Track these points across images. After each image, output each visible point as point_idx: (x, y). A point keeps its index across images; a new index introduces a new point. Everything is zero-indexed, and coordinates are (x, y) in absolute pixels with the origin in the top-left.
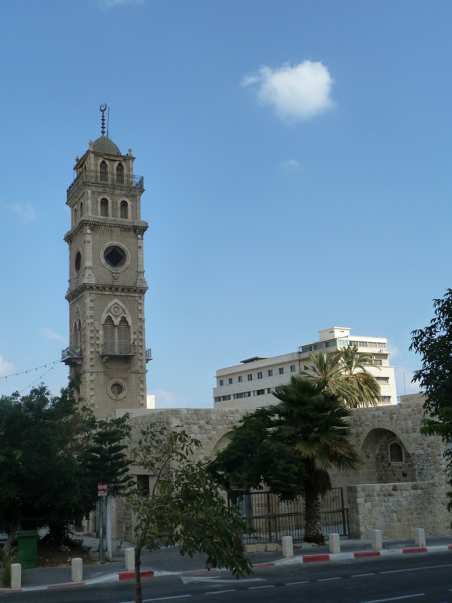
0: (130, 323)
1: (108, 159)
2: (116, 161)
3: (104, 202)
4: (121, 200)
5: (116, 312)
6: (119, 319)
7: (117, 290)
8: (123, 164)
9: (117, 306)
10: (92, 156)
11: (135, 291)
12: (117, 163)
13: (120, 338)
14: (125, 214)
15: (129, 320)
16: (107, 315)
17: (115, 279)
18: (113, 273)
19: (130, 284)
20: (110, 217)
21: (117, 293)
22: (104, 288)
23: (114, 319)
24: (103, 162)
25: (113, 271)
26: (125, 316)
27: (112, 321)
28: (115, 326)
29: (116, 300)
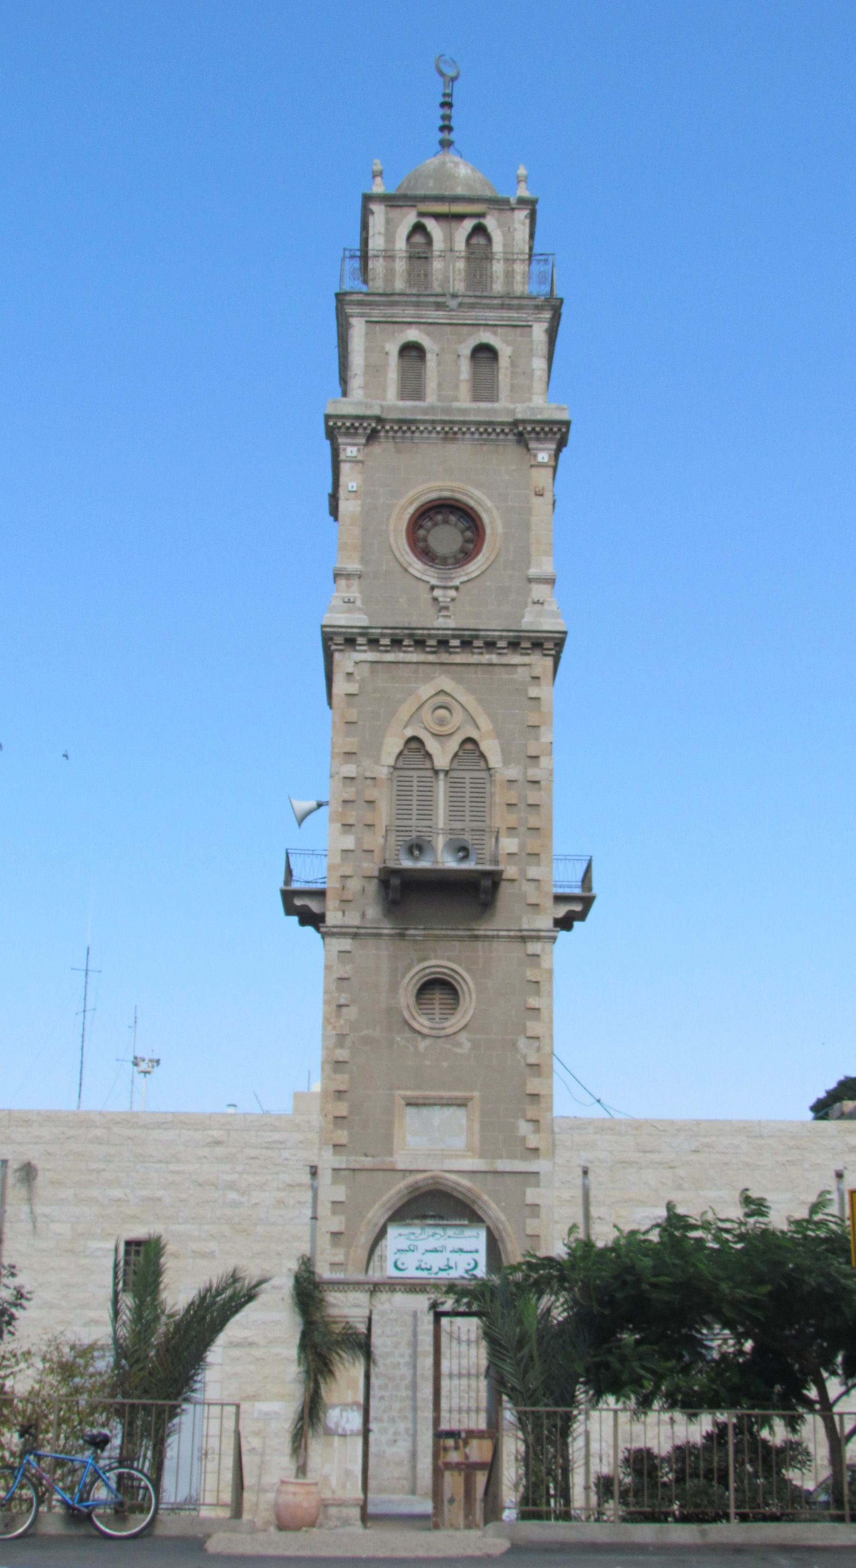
0: (495, 759)
1: (437, 217)
2: (460, 217)
3: (412, 352)
4: (473, 342)
5: (442, 722)
6: (453, 745)
7: (443, 643)
8: (490, 222)
9: (443, 703)
10: (378, 210)
11: (514, 645)
12: (468, 225)
13: (454, 811)
14: (485, 388)
15: (490, 747)
16: (409, 733)
17: (440, 610)
18: (433, 588)
19: (490, 620)
20: (431, 398)
21: (445, 658)
22: (397, 643)
23: (432, 745)
24: (419, 228)
25: (434, 582)
26: (475, 735)
27: (428, 756)
28: (436, 772)
29: (445, 682)
